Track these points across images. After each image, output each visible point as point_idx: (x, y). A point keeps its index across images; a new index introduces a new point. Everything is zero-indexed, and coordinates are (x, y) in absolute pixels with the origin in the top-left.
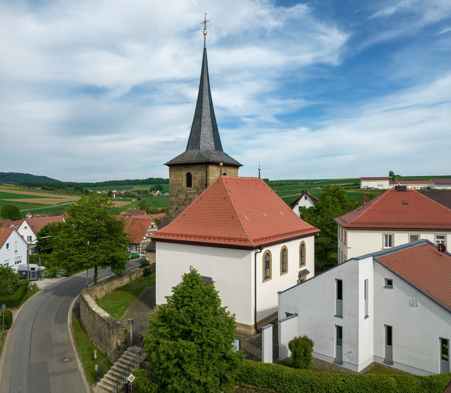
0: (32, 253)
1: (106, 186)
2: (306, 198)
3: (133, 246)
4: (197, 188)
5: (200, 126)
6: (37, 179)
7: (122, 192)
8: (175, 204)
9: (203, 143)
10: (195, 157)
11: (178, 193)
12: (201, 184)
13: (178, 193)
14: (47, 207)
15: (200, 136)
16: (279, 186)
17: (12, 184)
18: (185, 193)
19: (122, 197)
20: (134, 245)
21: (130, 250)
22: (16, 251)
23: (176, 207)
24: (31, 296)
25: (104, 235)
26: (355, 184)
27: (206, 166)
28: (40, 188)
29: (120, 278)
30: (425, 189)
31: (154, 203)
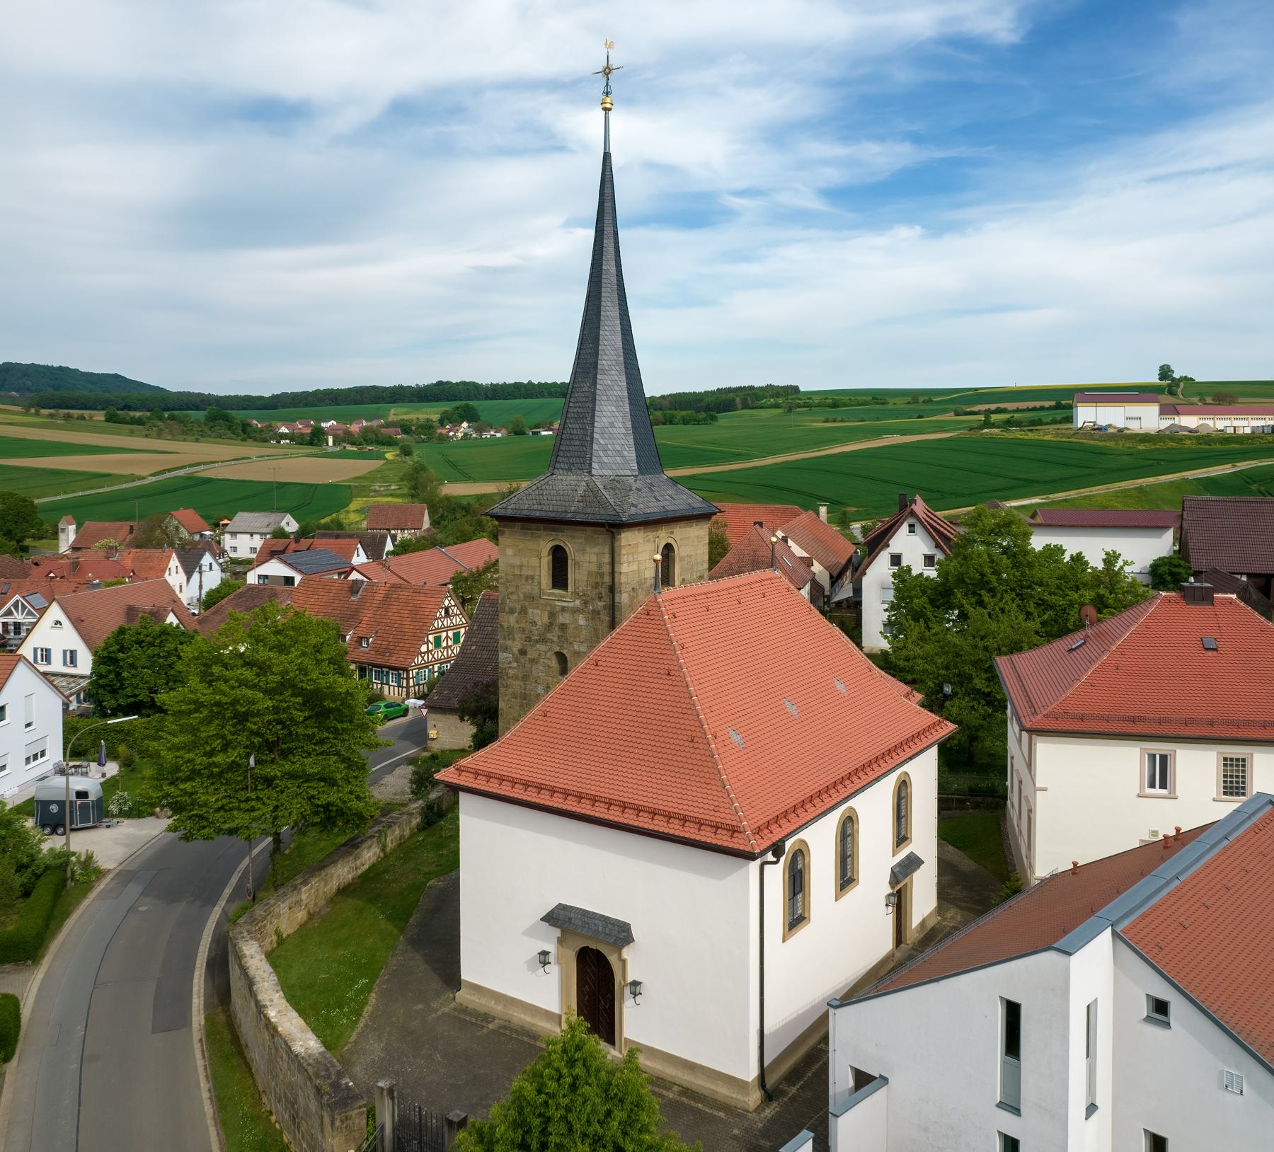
0: (79, 701)
1: (306, 406)
2: (912, 529)
3: (388, 673)
4: (584, 595)
5: (594, 401)
6: (93, 383)
7: (355, 428)
8: (517, 636)
9: (601, 453)
10: (577, 498)
11: (527, 604)
12: (597, 583)
13: (527, 604)
14: (124, 486)
15: (593, 432)
16: (829, 409)
17: (13, 402)
18: (548, 608)
19: (353, 444)
20: (391, 672)
21: (379, 686)
22: (28, 725)
23: (519, 646)
24: (79, 903)
25: (301, 730)
26: (1058, 406)
27: (613, 533)
28: (100, 416)
29: (351, 855)
30: (1266, 431)
31: (452, 465)
